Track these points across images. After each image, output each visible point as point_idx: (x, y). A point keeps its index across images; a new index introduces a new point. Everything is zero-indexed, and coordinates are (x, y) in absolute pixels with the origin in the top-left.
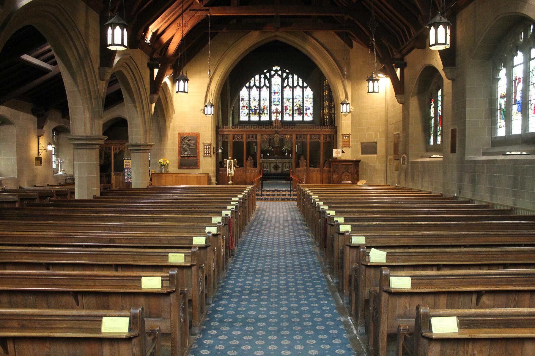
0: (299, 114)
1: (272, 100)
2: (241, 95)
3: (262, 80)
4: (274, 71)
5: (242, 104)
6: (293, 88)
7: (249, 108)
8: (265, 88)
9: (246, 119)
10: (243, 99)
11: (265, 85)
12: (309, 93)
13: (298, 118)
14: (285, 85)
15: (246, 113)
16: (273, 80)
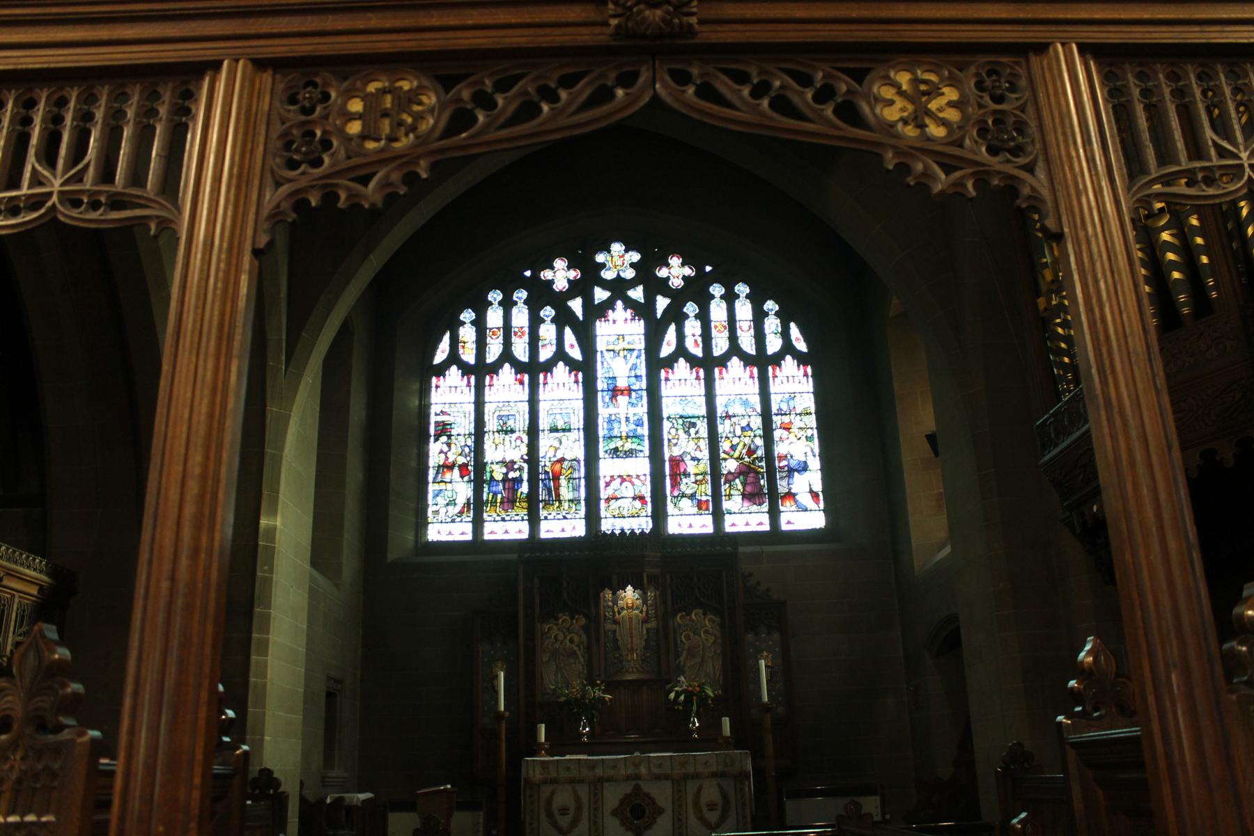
0: (751, 496)
1: (602, 432)
2: (434, 409)
3: (548, 331)
4: (605, 284)
5: (436, 451)
6: (708, 364)
7: (477, 471)
8: (561, 369)
9: (462, 531)
10: (444, 429)
11: (561, 355)
12: (795, 386)
13: (745, 518)
14: (667, 350)
15: (461, 501)
16: (601, 328)
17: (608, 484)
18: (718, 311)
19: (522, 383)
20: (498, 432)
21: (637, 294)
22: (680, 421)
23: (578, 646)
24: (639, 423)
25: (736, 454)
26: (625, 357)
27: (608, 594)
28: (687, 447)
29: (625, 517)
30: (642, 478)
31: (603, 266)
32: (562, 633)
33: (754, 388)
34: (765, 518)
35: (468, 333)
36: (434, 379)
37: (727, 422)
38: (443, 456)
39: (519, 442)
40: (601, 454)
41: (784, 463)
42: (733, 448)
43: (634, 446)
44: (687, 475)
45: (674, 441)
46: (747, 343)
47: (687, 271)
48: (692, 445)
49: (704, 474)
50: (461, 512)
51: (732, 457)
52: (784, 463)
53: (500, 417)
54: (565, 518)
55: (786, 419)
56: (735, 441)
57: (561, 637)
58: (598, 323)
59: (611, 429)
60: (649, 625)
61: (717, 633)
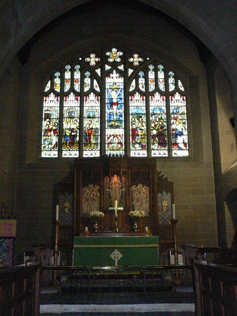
0: (162, 144)
2: (45, 109)
3: (87, 81)
4: (109, 63)
6: (147, 95)
9: (54, 154)
10: (48, 116)
11: (92, 90)
12: (179, 103)
13: (159, 152)
15: (54, 142)
16: (108, 80)
17: (108, 138)
18: (151, 75)
19: (77, 100)
20: (68, 118)
21: (121, 68)
22: (136, 115)
23: (96, 197)
24: (121, 116)
25: (157, 128)
26: (116, 91)
27: (107, 179)
28: (139, 125)
29: (114, 150)
30: (121, 136)
31: (109, 57)
32: (90, 192)
33: (163, 104)
34: (166, 152)
35: (57, 81)
36: (45, 98)
37: (153, 116)
38: (47, 126)
39: (76, 122)
40: (106, 127)
41: (174, 132)
42: (155, 126)
43: (119, 124)
44: (138, 135)
45: (134, 123)
46: (162, 87)
47: (140, 59)
48: (140, 124)
49: (144, 135)
50: (54, 147)
51: (155, 129)
52: (174, 132)
53: (69, 112)
54: (92, 150)
55: (176, 116)
56: (156, 123)
57: (90, 194)
58: (106, 78)
59: (110, 118)
60: (122, 190)
61: (148, 194)
